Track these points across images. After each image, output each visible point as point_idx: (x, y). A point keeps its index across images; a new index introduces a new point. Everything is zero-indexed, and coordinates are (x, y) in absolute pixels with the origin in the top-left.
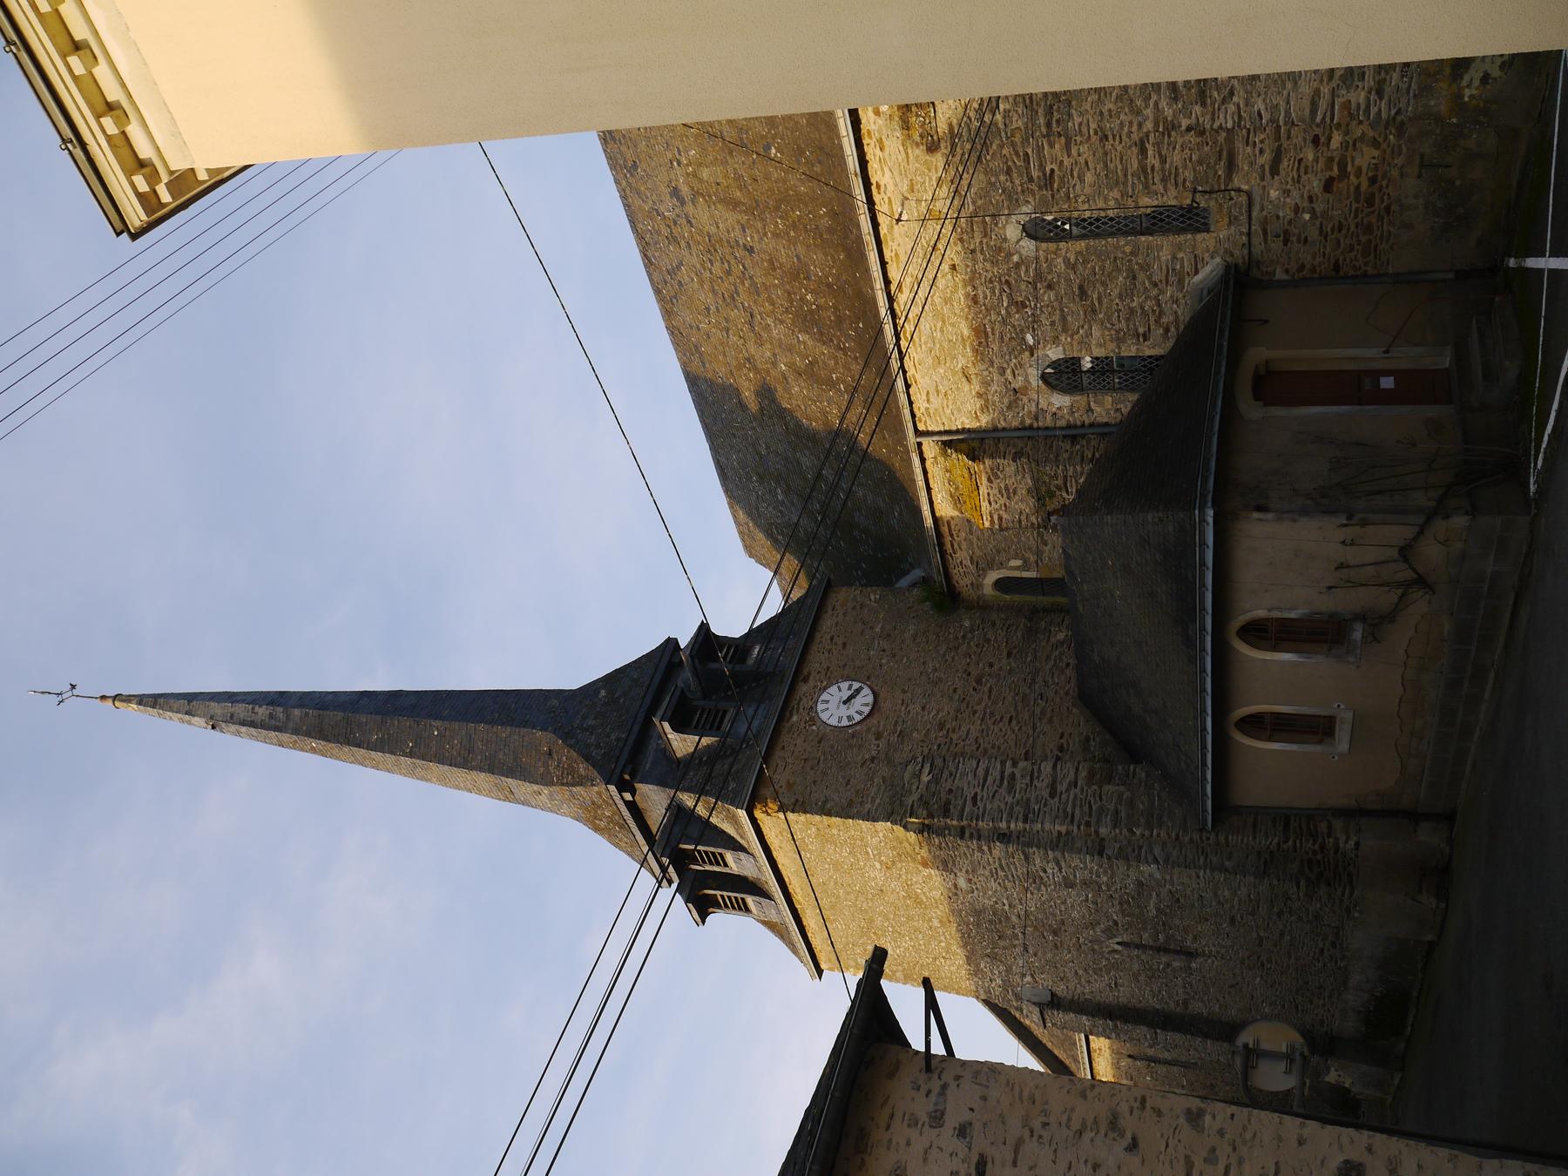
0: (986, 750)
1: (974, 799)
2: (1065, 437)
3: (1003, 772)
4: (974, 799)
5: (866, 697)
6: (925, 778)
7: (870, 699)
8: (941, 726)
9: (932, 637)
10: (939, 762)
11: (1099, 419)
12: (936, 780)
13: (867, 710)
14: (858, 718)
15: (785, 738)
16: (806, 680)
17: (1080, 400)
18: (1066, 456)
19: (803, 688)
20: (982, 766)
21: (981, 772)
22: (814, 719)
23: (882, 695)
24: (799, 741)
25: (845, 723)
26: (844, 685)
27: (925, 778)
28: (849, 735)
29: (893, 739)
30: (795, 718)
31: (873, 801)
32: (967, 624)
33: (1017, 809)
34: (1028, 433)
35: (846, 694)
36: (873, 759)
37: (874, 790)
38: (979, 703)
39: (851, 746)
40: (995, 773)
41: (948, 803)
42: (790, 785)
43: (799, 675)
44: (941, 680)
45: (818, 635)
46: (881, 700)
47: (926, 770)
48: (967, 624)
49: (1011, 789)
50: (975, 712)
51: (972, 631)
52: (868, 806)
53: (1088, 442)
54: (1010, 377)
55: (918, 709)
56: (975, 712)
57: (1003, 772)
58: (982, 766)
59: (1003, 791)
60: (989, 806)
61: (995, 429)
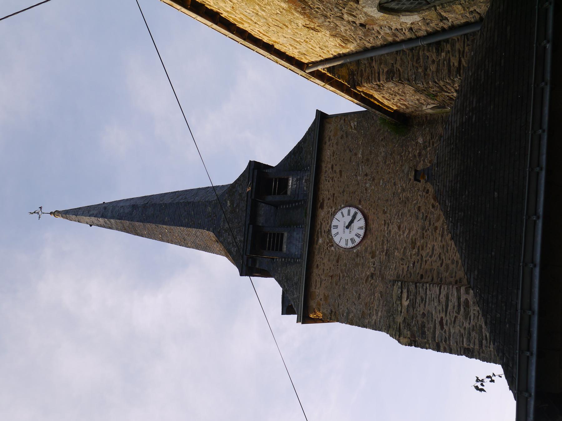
0: (447, 266)
1: (441, 323)
2: (429, 45)
3: (459, 298)
4: (441, 323)
5: (360, 222)
6: (406, 303)
7: (362, 223)
8: (413, 244)
9: (398, 158)
10: (412, 287)
11: (457, 22)
12: (412, 305)
13: (362, 232)
14: (358, 240)
15: (317, 258)
16: (322, 207)
17: (430, 14)
18: (433, 68)
19: (322, 214)
20: (444, 293)
21: (443, 299)
22: (331, 242)
23: (371, 217)
24: (326, 261)
25: (350, 245)
26: (345, 211)
27: (406, 303)
28: (355, 254)
29: (383, 257)
30: (320, 241)
31: (377, 314)
32: (420, 140)
33: (473, 334)
34: (394, 49)
35: (348, 219)
36: (372, 275)
37: (376, 303)
38: (438, 220)
39: (357, 265)
40: (454, 300)
41: (423, 326)
42: (326, 298)
43: (317, 205)
44: (407, 199)
45: (324, 165)
46: (371, 222)
47: (405, 295)
48: (420, 140)
49: (467, 315)
50: (436, 228)
51: (425, 148)
52: (374, 317)
53: (453, 45)
54: (351, 19)
55: (396, 229)
56: (436, 228)
57: (459, 298)
58: (444, 293)
59: (460, 317)
60: (452, 331)
61: (366, 50)
